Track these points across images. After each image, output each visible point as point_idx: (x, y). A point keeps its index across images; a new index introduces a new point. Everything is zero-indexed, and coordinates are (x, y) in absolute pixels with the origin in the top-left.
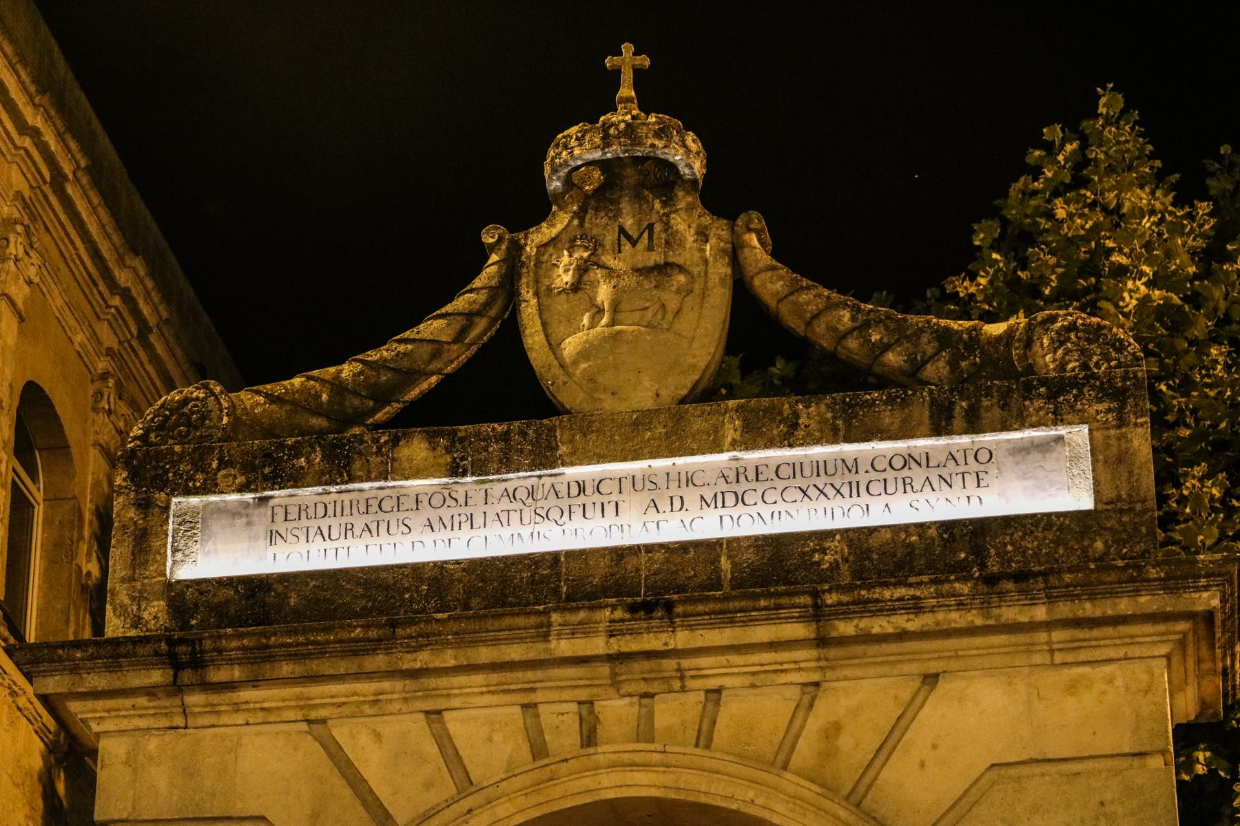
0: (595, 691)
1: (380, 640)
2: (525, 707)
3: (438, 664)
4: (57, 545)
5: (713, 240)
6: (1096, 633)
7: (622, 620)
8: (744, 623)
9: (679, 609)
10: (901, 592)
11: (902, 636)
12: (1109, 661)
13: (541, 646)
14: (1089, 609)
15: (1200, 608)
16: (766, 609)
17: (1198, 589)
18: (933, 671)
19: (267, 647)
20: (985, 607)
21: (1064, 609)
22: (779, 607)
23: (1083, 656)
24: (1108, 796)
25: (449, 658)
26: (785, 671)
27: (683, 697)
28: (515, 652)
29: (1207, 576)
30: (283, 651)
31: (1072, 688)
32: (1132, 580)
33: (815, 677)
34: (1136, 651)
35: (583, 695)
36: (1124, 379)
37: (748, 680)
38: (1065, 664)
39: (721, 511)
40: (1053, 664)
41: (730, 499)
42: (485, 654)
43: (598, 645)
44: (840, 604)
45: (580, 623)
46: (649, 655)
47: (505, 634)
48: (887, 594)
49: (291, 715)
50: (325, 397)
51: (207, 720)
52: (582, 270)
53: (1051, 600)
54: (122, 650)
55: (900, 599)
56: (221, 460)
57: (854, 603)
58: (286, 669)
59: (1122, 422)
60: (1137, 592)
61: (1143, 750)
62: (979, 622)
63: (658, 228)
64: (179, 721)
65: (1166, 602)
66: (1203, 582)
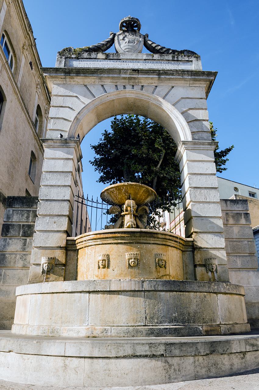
0: (125, 84)
1: (96, 72)
2: (115, 86)
3: (104, 76)
4: (40, 126)
5: (141, 36)
6: (196, 82)
7: (131, 72)
8: (149, 75)
9: (140, 71)
10: (171, 72)
11: (170, 79)
12: (197, 87)
13: (119, 75)
14: (196, 77)
15: (211, 79)
16: (152, 72)
17: (211, 76)
18: (173, 86)
19: (79, 71)
20: (182, 76)
21: (193, 77)
22: (154, 72)
23: (194, 85)
24: (197, 103)
25: (106, 76)
26: (153, 83)
27: (138, 86)
28: (116, 76)
29: (213, 74)
30: (81, 72)
31: (192, 89)
32: (203, 74)
33: (157, 85)
34: (201, 85)
35: (124, 84)
36: (198, 56)
37: (147, 84)
38: (191, 86)
39: (143, 66)
40: (190, 86)
41: (144, 65)
42: (111, 76)
43: (128, 76)
44: (162, 73)
45: (125, 72)
46: (134, 78)
47: (114, 73)
48: (169, 72)
49: (81, 83)
50: (87, 49)
51: (70, 83)
52: (124, 37)
53: (191, 76)
54: (58, 70)
55: (171, 73)
56: (72, 53)
57: (165, 73)
58: (82, 75)
59: (197, 61)
60: (203, 76)
61: (202, 97)
62: (181, 77)
63: (134, 34)
64: (65, 82)
65: (207, 78)
66: (212, 75)
